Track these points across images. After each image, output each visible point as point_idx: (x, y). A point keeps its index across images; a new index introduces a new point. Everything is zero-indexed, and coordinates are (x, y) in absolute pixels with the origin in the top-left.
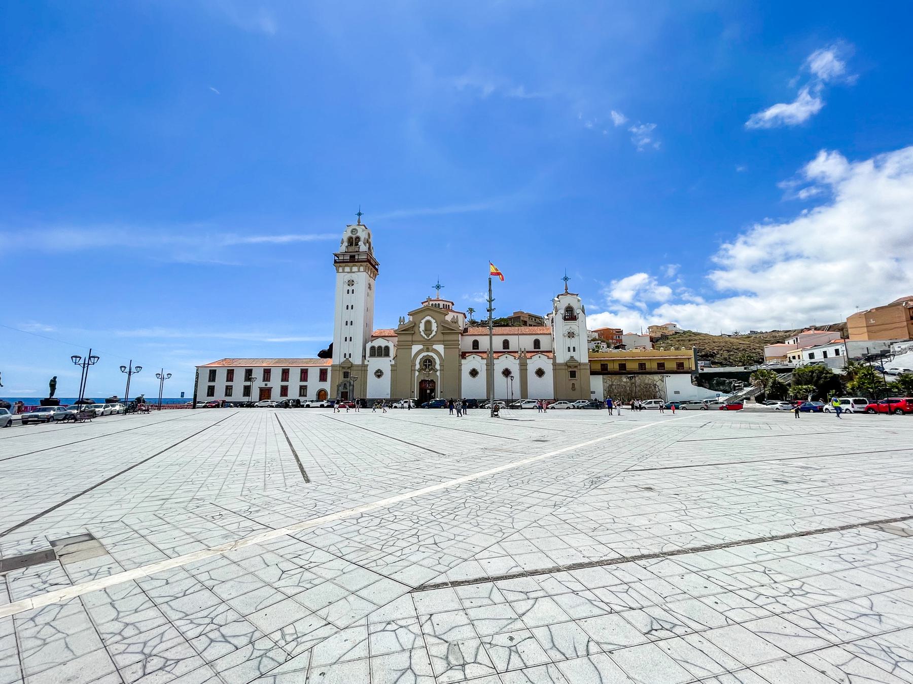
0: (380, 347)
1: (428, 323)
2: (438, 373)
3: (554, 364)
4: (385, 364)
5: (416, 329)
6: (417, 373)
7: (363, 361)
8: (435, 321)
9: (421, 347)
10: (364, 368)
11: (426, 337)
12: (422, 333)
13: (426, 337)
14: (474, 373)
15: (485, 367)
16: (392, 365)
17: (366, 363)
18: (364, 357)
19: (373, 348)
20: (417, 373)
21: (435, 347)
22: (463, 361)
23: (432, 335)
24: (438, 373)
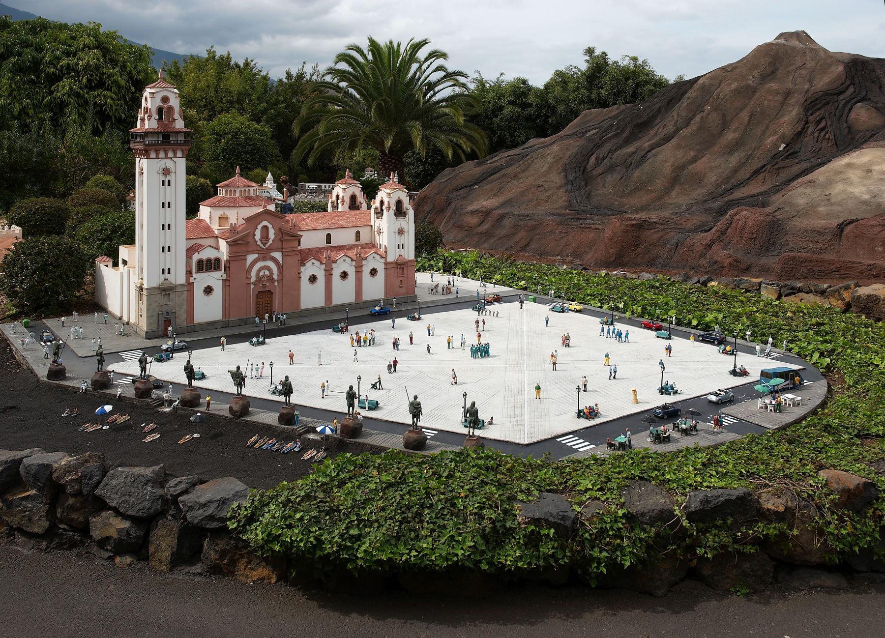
0: (209, 260)
1: (265, 228)
2: (276, 284)
3: (386, 264)
4: (215, 279)
5: (250, 239)
6: (252, 286)
7: (188, 279)
8: (271, 226)
9: (256, 256)
10: (190, 286)
11: (263, 247)
12: (259, 243)
13: (263, 247)
14: (313, 279)
15: (323, 273)
16: (224, 280)
17: (192, 280)
18: (189, 273)
19: (200, 262)
20: (252, 286)
21: (273, 254)
22: (302, 269)
23: (268, 245)
24: (276, 284)
